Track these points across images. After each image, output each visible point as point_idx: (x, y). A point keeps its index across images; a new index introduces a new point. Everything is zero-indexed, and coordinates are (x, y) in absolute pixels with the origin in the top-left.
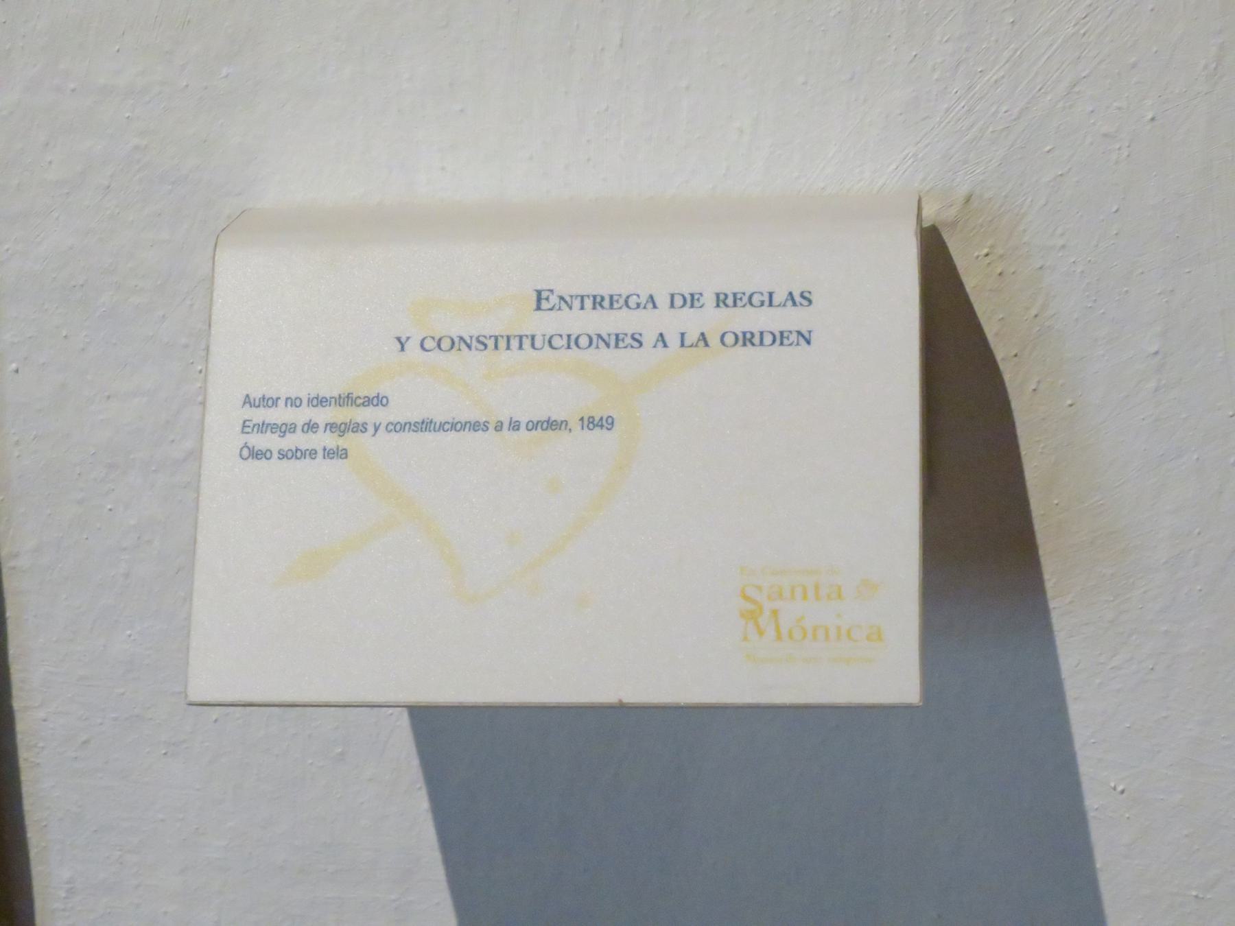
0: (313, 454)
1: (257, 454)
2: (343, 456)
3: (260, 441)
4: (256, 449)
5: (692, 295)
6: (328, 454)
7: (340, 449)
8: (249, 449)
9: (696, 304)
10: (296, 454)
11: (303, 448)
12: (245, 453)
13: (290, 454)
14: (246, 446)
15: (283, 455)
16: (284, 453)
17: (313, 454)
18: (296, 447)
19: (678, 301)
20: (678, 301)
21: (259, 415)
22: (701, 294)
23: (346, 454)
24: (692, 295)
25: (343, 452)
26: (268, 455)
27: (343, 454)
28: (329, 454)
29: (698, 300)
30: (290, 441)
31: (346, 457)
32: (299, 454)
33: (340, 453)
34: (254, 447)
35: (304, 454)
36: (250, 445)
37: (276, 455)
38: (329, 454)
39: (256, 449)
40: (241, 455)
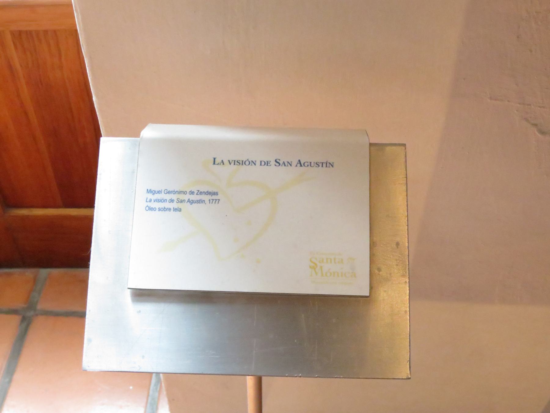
0: (170, 209)
1: (151, 209)
2: (180, 211)
4: (151, 207)
5: (267, 162)
6: (175, 210)
7: (179, 208)
8: (148, 207)
9: (269, 164)
10: (165, 209)
11: (166, 207)
13: (162, 209)
14: (147, 206)
15: (160, 209)
16: (160, 209)
17: (170, 209)
18: (164, 207)
19: (263, 163)
20: (263, 163)
22: (270, 161)
23: (181, 210)
24: (267, 162)
27: (180, 210)
28: (175, 210)
29: (269, 163)
30: (161, 205)
31: (181, 211)
32: (165, 210)
34: (150, 207)
35: (167, 210)
36: (149, 206)
37: (157, 209)
38: (175, 210)
39: (151, 207)
40: (146, 210)
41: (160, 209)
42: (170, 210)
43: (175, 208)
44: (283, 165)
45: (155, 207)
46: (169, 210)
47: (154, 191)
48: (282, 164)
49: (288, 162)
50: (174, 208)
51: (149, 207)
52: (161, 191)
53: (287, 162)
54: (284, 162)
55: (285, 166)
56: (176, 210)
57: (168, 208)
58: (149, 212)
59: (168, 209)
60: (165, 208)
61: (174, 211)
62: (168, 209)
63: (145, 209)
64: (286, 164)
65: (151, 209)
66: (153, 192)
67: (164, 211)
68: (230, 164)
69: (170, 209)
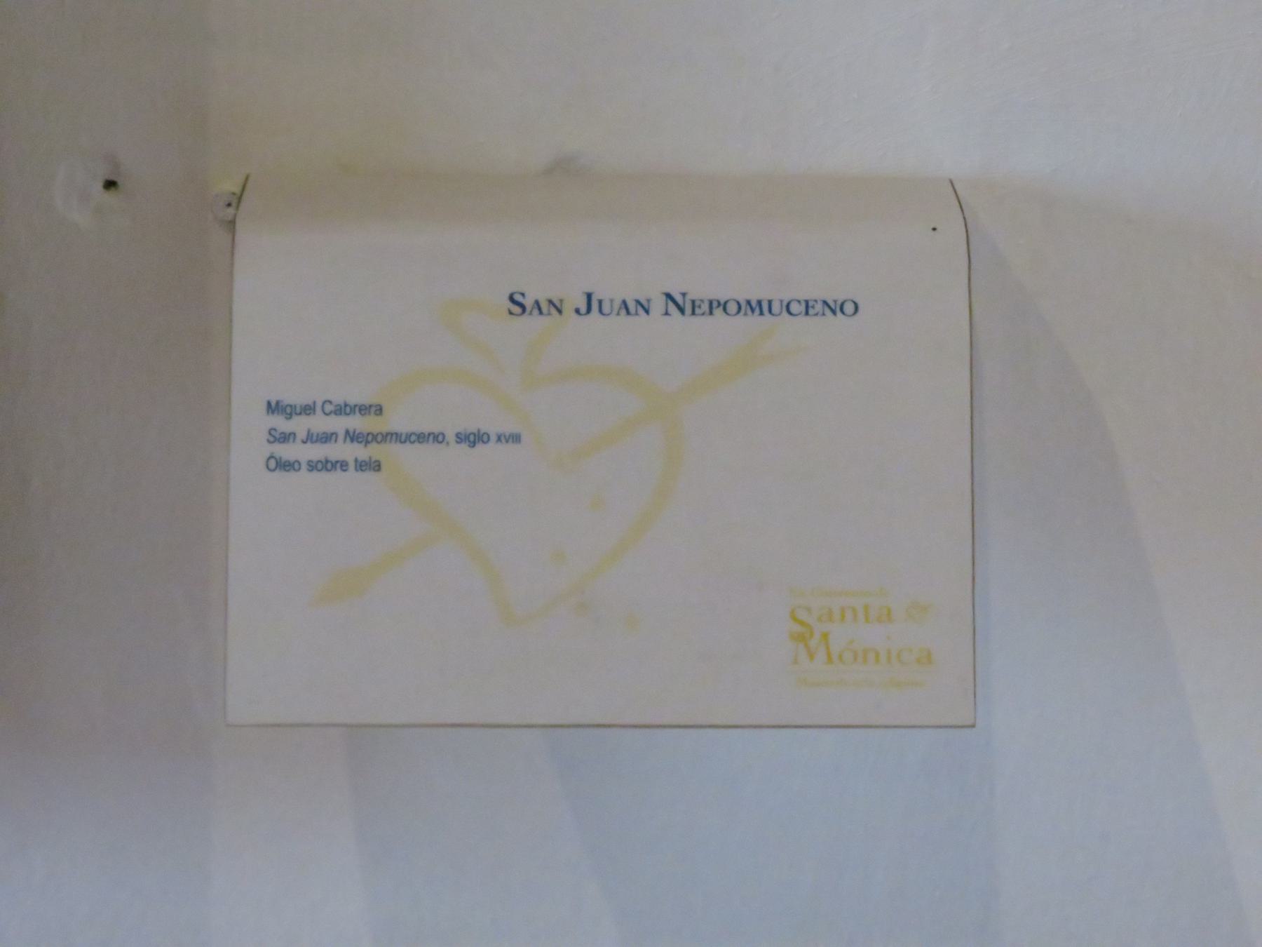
0: (343, 465)
4: (283, 461)
6: (361, 466)
8: (276, 459)
13: (320, 466)
14: (271, 457)
15: (313, 466)
16: (314, 464)
17: (343, 465)
23: (379, 466)
27: (376, 466)
33: (373, 465)
37: (304, 466)
38: (361, 466)
40: (268, 467)
41: (313, 466)
42: (344, 468)
46: (342, 466)
47: (291, 406)
48: (620, 308)
49: (638, 302)
50: (356, 460)
52: (312, 406)
53: (634, 303)
54: (624, 302)
60: (327, 461)
63: (265, 467)
64: (632, 306)
65: (285, 466)
66: (288, 410)
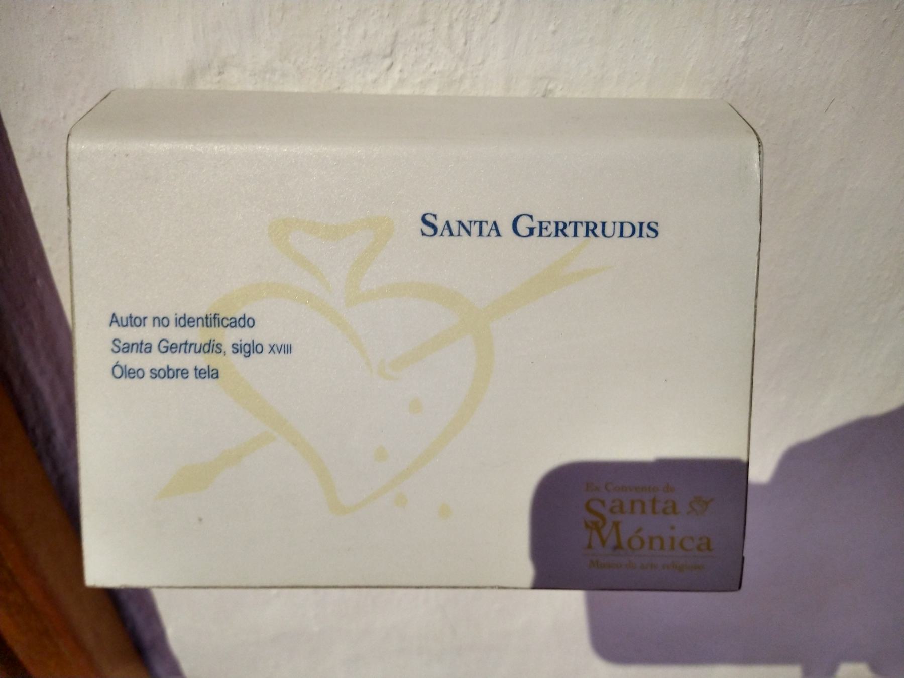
0: (184, 373)
1: (129, 373)
2: (215, 376)
3: (133, 360)
4: (127, 369)
6: (200, 373)
7: (211, 370)
8: (121, 367)
10: (169, 373)
11: (174, 366)
12: (118, 371)
13: (162, 374)
15: (155, 374)
16: (157, 372)
17: (184, 373)
18: (168, 367)
21: (130, 335)
23: (217, 373)
25: (215, 371)
26: (140, 373)
27: (214, 374)
28: (200, 373)
31: (217, 377)
33: (211, 373)
34: (125, 366)
35: (175, 375)
36: (122, 363)
37: (148, 374)
38: (200, 373)
39: (127, 369)
41: (155, 374)
42: (185, 376)
43: (199, 368)
44: (447, 232)
45: (142, 367)
46: (182, 374)
50: (196, 369)
51: (123, 367)
53: (457, 224)
55: (451, 234)
56: (203, 376)
57: (178, 370)
58: (125, 382)
59: (180, 372)
60: (169, 370)
61: (197, 378)
62: (180, 372)
64: (454, 226)
65: (129, 373)
67: (169, 377)
68: (495, 223)
69: (185, 371)
